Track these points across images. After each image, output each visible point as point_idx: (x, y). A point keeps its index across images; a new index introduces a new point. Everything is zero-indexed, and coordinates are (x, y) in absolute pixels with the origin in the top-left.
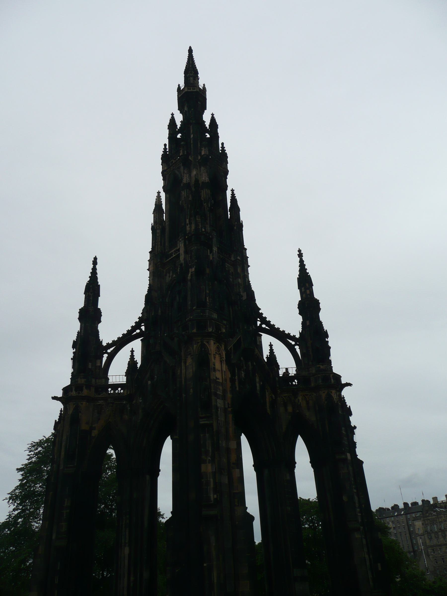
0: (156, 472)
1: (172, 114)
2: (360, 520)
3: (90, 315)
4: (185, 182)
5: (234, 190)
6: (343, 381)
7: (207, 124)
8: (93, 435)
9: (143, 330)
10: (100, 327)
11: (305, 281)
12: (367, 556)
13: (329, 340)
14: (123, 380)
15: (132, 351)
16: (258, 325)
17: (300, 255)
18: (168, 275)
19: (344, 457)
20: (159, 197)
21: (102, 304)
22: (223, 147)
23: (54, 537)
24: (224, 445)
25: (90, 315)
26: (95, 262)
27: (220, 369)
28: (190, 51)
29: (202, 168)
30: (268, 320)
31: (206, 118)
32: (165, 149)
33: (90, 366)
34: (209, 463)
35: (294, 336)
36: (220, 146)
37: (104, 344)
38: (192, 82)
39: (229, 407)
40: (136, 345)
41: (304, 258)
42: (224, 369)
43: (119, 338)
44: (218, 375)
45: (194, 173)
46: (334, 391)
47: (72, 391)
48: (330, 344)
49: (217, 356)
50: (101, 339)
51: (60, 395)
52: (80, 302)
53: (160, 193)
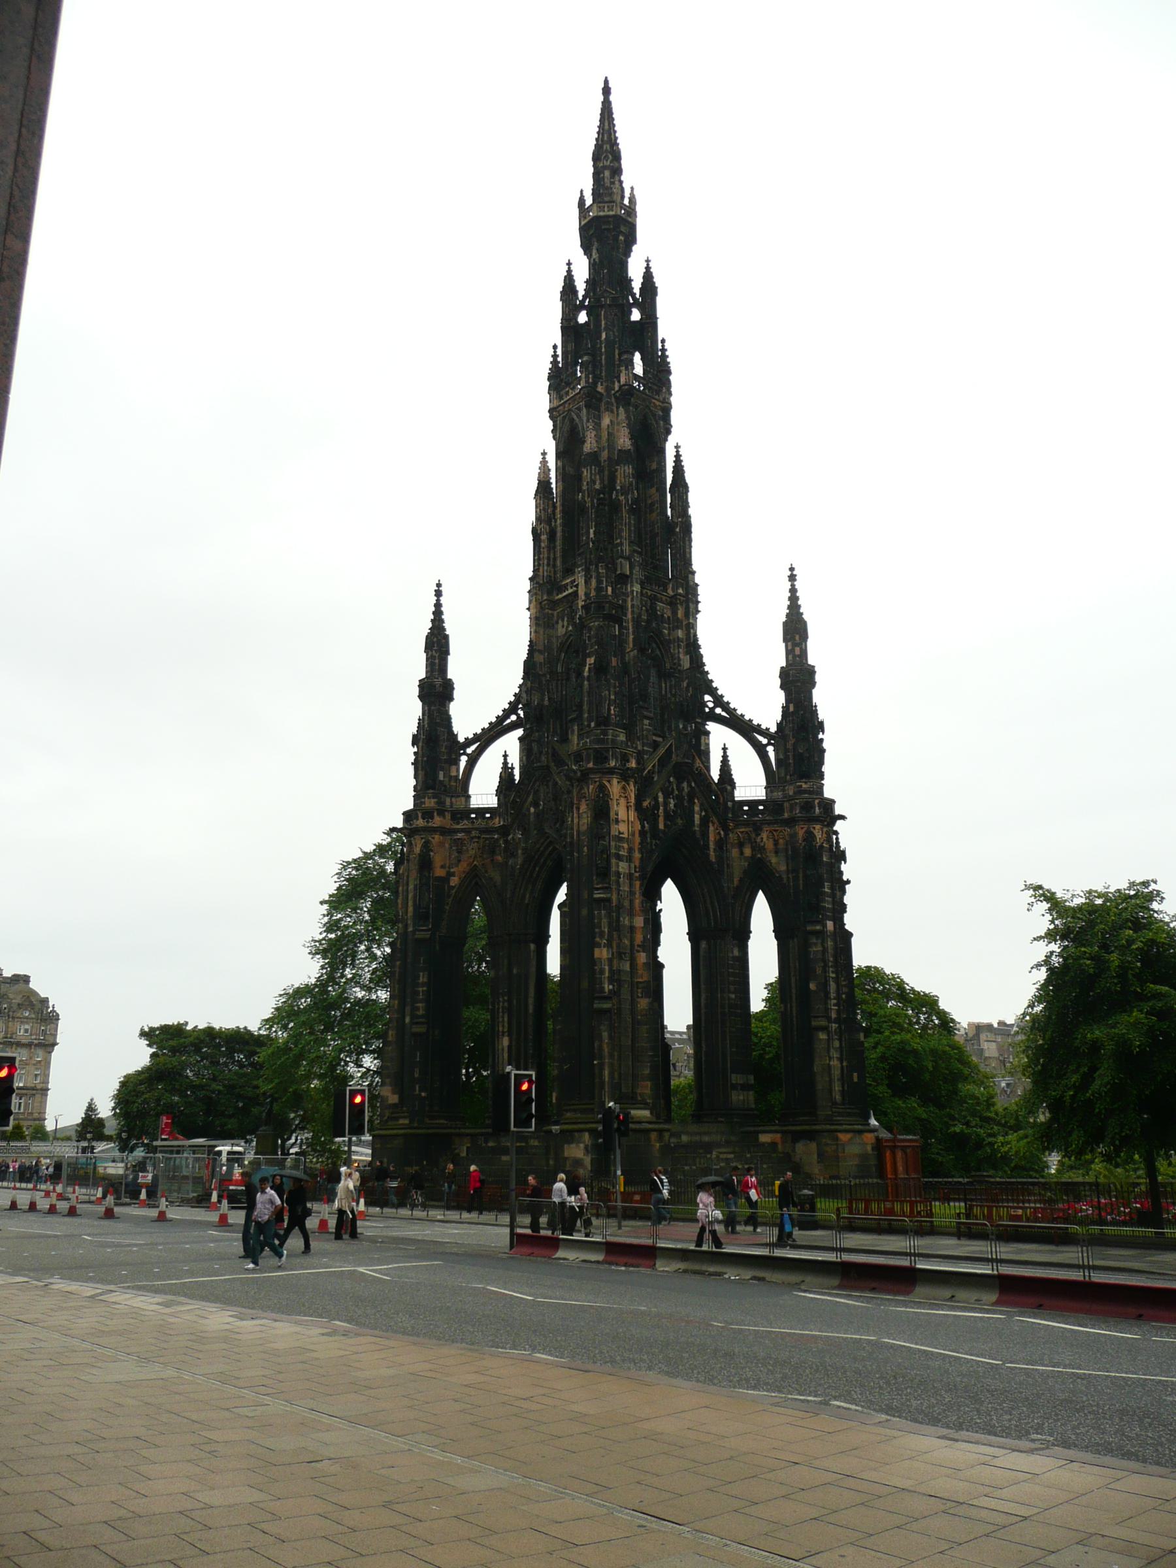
0: (544, 938)
3: (436, 691)
6: (837, 812)
7: (637, 286)
8: (452, 884)
10: (454, 709)
11: (795, 630)
14: (492, 801)
15: (505, 756)
19: (818, 928)
20: (544, 462)
21: (455, 670)
23: (407, 1020)
24: (627, 922)
28: (606, 91)
32: (555, 356)
33: (441, 777)
35: (767, 729)
37: (461, 739)
38: (607, 182)
42: (632, 818)
44: (623, 827)
45: (606, 421)
46: (818, 827)
48: (825, 745)
50: (455, 730)
52: (419, 669)
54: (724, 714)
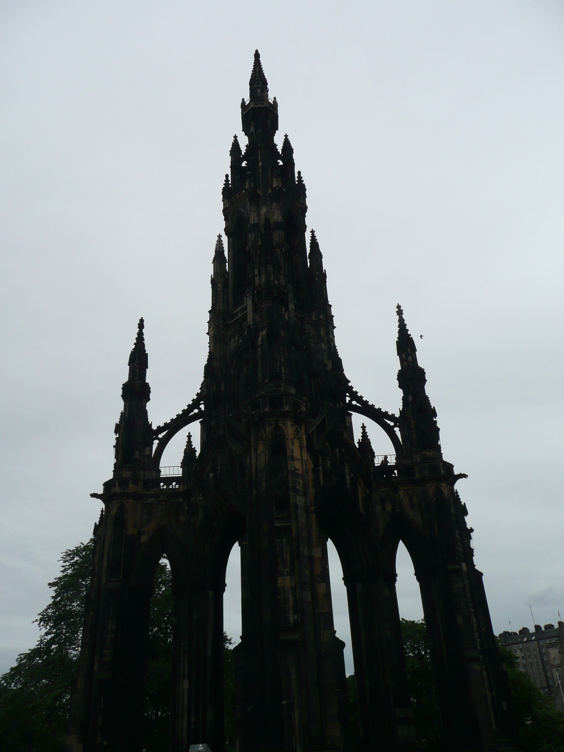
0: (221, 586)
1: (235, 137)
2: (479, 647)
3: (136, 391)
4: (252, 222)
5: (314, 232)
6: (456, 472)
7: (280, 148)
8: (142, 541)
9: (203, 409)
10: (149, 406)
11: (406, 346)
12: (488, 693)
13: (437, 419)
14: (178, 472)
15: (189, 436)
16: (347, 402)
18: (233, 340)
19: (457, 567)
20: (220, 242)
21: (150, 378)
22: (300, 177)
23: (96, 667)
24: (306, 553)
25: (136, 391)
26: (141, 325)
27: (299, 457)
28: (257, 55)
29: (274, 204)
30: (359, 395)
31: (279, 141)
32: (227, 181)
33: (137, 455)
34: (287, 575)
36: (296, 175)
37: (154, 427)
38: (259, 95)
39: (311, 505)
40: (194, 428)
42: (305, 457)
43: (172, 420)
44: (298, 465)
45: (264, 210)
46: (444, 485)
47: (115, 486)
48: (438, 425)
49: (296, 441)
50: (150, 421)
51: (100, 491)
52: (123, 375)
53: (221, 236)
54: (358, 405)
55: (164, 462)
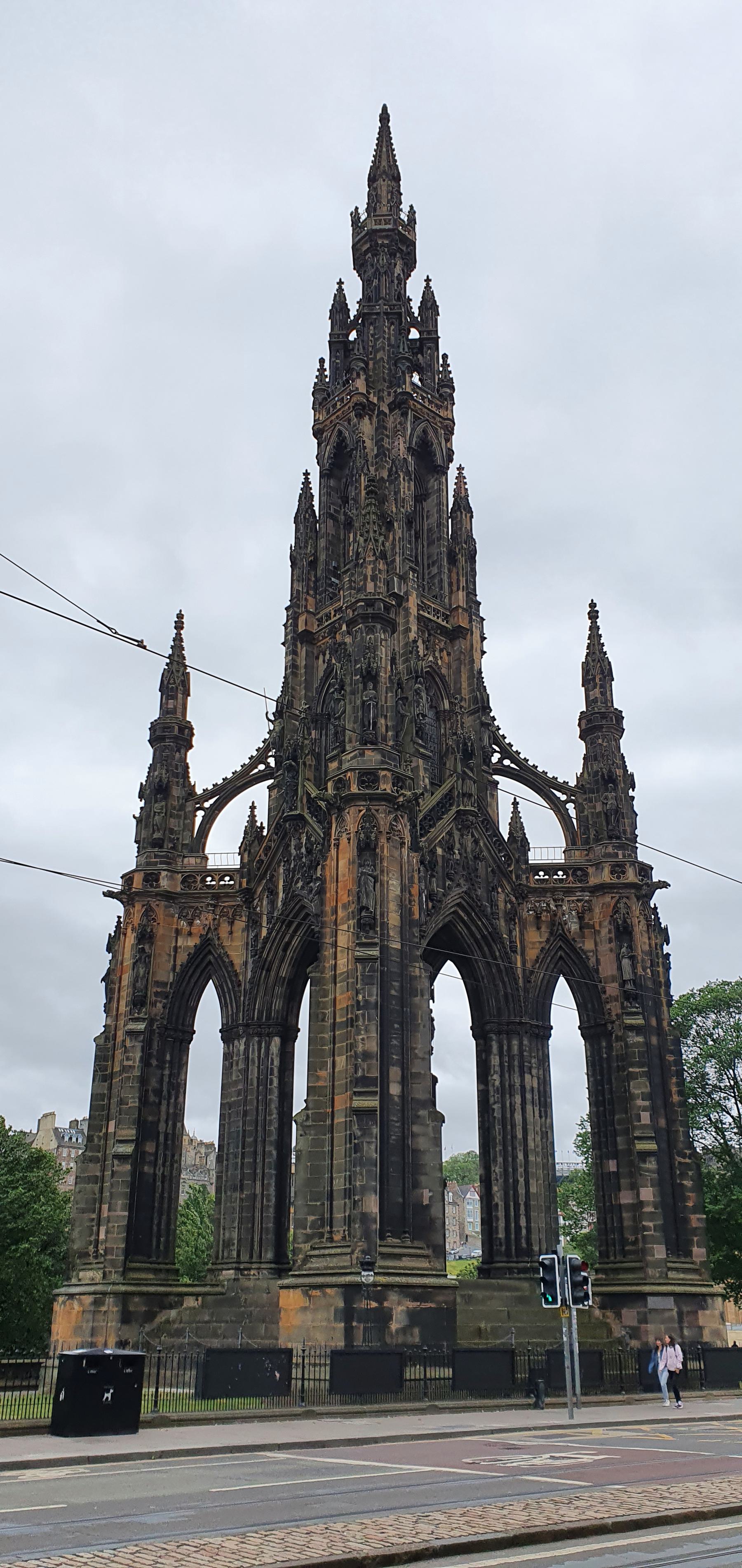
9: (273, 764)
11: (597, 671)
15: (253, 808)
17: (593, 615)
18: (321, 657)
26: (179, 625)
37: (199, 791)
40: (259, 795)
41: (599, 622)
54: (513, 766)
55: (211, 846)
